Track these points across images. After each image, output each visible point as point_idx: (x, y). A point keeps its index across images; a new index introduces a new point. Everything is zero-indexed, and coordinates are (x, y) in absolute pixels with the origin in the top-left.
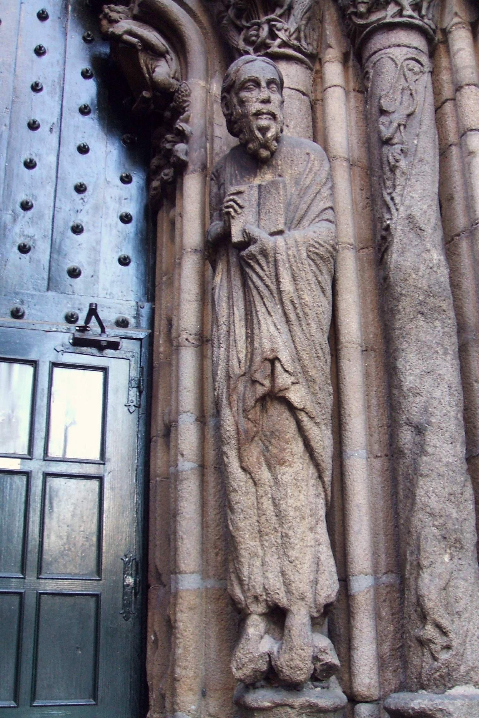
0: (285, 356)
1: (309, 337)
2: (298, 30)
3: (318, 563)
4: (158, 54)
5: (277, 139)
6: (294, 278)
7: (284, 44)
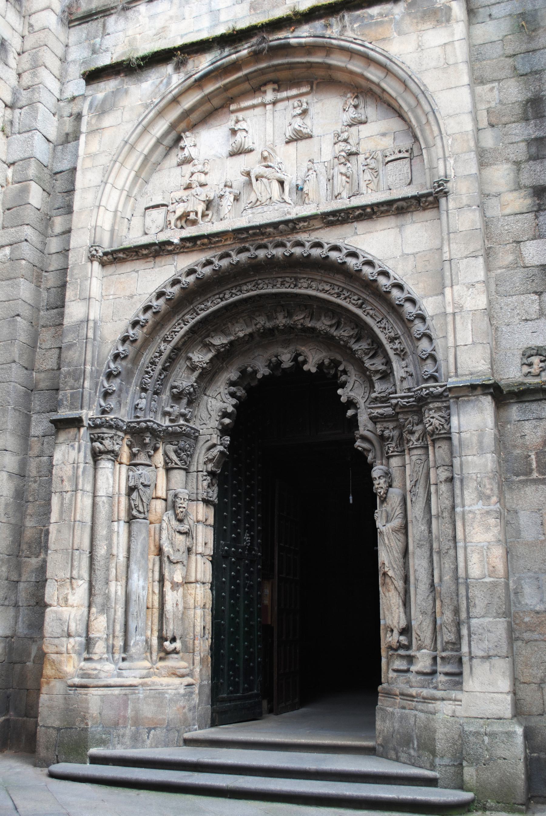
0: (386, 563)
1: (393, 556)
2: (396, 445)
3: (399, 617)
4: (369, 451)
5: (384, 493)
6: (388, 539)
7: (392, 452)
